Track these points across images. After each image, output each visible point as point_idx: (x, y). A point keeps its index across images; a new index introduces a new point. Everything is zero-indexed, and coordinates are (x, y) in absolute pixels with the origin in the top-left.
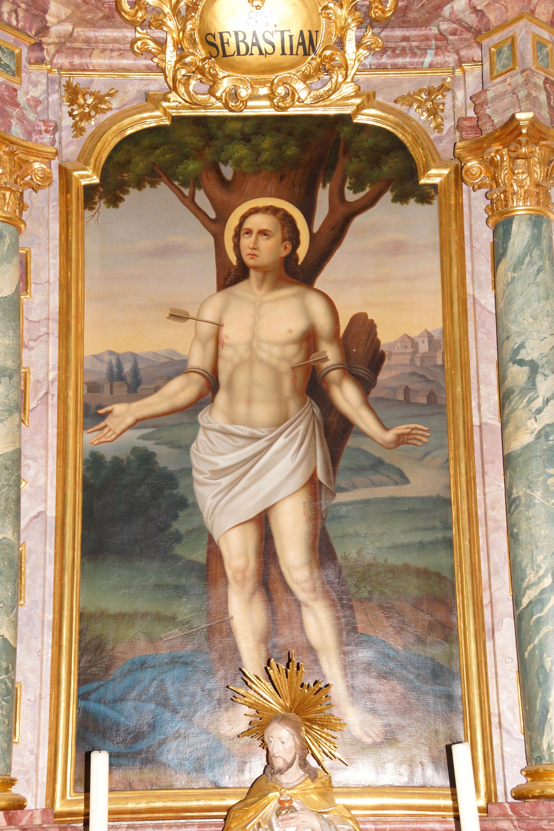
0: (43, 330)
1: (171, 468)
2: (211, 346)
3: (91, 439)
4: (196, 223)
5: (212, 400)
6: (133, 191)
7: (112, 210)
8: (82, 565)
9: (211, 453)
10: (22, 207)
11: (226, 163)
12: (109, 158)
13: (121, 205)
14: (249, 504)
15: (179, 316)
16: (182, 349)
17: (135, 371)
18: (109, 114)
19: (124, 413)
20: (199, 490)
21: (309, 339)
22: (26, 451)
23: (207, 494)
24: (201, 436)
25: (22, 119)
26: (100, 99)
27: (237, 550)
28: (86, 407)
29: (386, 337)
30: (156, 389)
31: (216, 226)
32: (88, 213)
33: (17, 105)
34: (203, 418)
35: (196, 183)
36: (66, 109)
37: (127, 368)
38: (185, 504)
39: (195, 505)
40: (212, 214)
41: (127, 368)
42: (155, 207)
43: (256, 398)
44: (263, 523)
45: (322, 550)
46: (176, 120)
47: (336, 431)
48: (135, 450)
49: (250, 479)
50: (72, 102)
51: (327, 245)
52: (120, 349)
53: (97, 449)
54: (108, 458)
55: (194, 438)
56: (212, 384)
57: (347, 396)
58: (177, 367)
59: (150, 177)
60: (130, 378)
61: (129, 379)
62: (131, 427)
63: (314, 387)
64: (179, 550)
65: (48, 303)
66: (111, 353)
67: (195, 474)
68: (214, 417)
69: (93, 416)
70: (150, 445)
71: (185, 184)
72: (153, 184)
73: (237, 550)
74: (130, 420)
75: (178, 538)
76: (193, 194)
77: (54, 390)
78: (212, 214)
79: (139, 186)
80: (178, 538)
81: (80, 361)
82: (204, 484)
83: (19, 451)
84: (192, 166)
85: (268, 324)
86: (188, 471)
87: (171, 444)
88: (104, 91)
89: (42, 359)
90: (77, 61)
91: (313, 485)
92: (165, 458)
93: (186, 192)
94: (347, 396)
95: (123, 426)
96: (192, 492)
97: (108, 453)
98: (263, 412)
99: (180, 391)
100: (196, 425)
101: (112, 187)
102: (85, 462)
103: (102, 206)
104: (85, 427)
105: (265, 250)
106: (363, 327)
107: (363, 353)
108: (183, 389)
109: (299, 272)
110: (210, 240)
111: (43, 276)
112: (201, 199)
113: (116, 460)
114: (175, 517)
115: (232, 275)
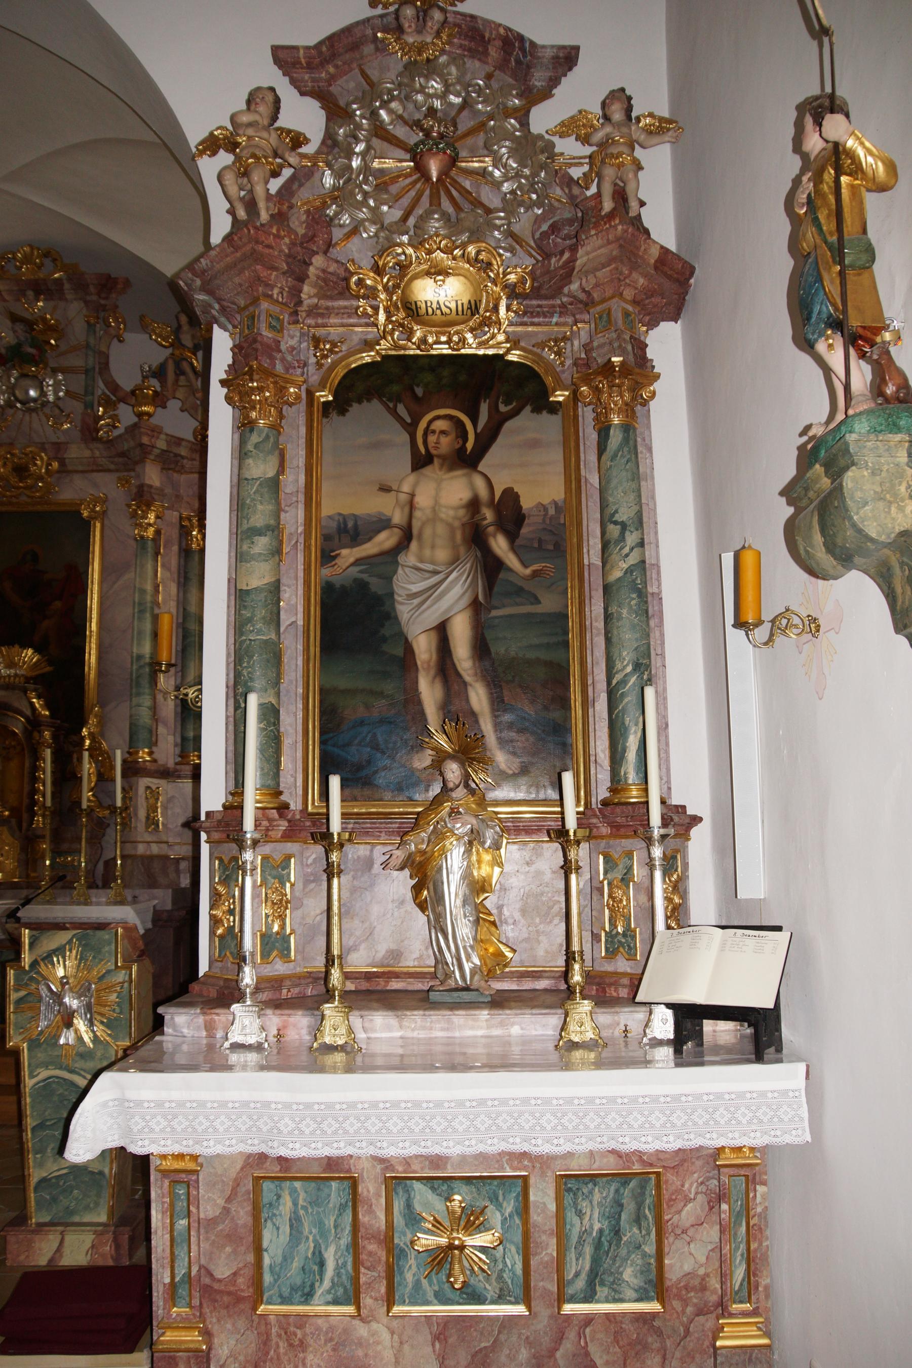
0: (295, 499)
1: (380, 593)
2: (407, 510)
3: (326, 572)
4: (398, 426)
5: (408, 546)
6: (355, 405)
7: (341, 418)
8: (321, 656)
9: (407, 582)
10: (281, 416)
11: (418, 386)
12: (340, 383)
13: (347, 414)
14: (431, 616)
15: (385, 489)
16: (387, 512)
17: (356, 526)
18: (340, 355)
19: (348, 555)
20: (399, 607)
21: (474, 505)
22: (284, 580)
23: (404, 611)
24: (400, 571)
25: (283, 360)
26: (334, 344)
27: (424, 648)
28: (323, 551)
29: (527, 503)
30: (370, 539)
31: (410, 429)
32: (325, 420)
33: (280, 351)
34: (401, 558)
35: (398, 399)
36: (312, 352)
37: (350, 524)
38: (389, 616)
39: (396, 618)
40: (409, 420)
41: (350, 524)
42: (370, 414)
43: (437, 545)
44: (442, 630)
45: (481, 647)
46: (386, 358)
47: (491, 567)
48: (355, 580)
49: (434, 602)
50: (316, 347)
52: (345, 512)
53: (330, 579)
54: (338, 586)
55: (395, 572)
56: (407, 535)
57: (500, 545)
58: (384, 524)
59: (367, 396)
60: (351, 531)
61: (351, 532)
62: (353, 564)
63: (476, 537)
64: (385, 648)
65: (297, 481)
66: (340, 514)
67: (396, 597)
68: (409, 558)
69: (327, 557)
70: (365, 577)
71: (390, 400)
72: (369, 400)
73: (424, 648)
74: (352, 560)
75: (384, 640)
76: (396, 406)
77: (301, 540)
78: (409, 420)
79: (360, 402)
80: (384, 640)
81: (318, 520)
82: (402, 604)
83: (278, 581)
84: (395, 388)
85: (446, 494)
86: (391, 594)
87: (379, 576)
88: (337, 339)
89: (294, 519)
90: (320, 321)
91: (476, 606)
92: (376, 586)
93: (391, 405)
94: (500, 545)
95: (347, 564)
96: (394, 609)
97: (337, 581)
98: (442, 555)
99: (385, 540)
100: (396, 563)
101: (340, 404)
102: (322, 589)
103: (334, 415)
104: (322, 565)
105: (445, 444)
106: (511, 496)
108: (388, 539)
109: (467, 460)
110: (406, 437)
111: (295, 463)
112: (401, 410)
113: (343, 586)
114: (383, 626)
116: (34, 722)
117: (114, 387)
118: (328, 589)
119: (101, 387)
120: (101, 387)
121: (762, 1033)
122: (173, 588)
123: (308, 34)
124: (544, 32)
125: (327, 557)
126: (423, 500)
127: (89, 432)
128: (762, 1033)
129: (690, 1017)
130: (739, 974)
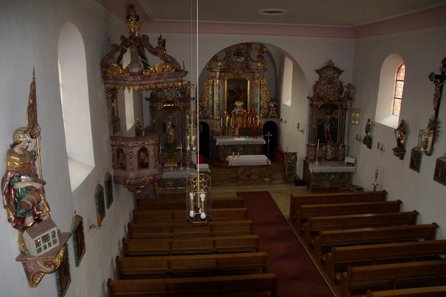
9: (325, 125)
19: (320, 122)
27: (326, 130)
44: (327, 129)
47: (332, 124)
49: (327, 127)
51: (332, 112)
56: (325, 121)
57: (333, 122)
60: (320, 120)
63: (331, 121)
73: (326, 130)
85: (329, 117)
91: (330, 127)
94: (333, 122)
99: (323, 121)
106: (334, 117)
107: (334, 119)
109: (330, 114)
115: (327, 114)
116: (244, 113)
117: (251, 59)
118: (318, 125)
119: (249, 59)
123: (318, 68)
124: (341, 68)
125: (318, 122)
127: (247, 67)
128: (353, 165)
129: (348, 163)
130: (352, 161)
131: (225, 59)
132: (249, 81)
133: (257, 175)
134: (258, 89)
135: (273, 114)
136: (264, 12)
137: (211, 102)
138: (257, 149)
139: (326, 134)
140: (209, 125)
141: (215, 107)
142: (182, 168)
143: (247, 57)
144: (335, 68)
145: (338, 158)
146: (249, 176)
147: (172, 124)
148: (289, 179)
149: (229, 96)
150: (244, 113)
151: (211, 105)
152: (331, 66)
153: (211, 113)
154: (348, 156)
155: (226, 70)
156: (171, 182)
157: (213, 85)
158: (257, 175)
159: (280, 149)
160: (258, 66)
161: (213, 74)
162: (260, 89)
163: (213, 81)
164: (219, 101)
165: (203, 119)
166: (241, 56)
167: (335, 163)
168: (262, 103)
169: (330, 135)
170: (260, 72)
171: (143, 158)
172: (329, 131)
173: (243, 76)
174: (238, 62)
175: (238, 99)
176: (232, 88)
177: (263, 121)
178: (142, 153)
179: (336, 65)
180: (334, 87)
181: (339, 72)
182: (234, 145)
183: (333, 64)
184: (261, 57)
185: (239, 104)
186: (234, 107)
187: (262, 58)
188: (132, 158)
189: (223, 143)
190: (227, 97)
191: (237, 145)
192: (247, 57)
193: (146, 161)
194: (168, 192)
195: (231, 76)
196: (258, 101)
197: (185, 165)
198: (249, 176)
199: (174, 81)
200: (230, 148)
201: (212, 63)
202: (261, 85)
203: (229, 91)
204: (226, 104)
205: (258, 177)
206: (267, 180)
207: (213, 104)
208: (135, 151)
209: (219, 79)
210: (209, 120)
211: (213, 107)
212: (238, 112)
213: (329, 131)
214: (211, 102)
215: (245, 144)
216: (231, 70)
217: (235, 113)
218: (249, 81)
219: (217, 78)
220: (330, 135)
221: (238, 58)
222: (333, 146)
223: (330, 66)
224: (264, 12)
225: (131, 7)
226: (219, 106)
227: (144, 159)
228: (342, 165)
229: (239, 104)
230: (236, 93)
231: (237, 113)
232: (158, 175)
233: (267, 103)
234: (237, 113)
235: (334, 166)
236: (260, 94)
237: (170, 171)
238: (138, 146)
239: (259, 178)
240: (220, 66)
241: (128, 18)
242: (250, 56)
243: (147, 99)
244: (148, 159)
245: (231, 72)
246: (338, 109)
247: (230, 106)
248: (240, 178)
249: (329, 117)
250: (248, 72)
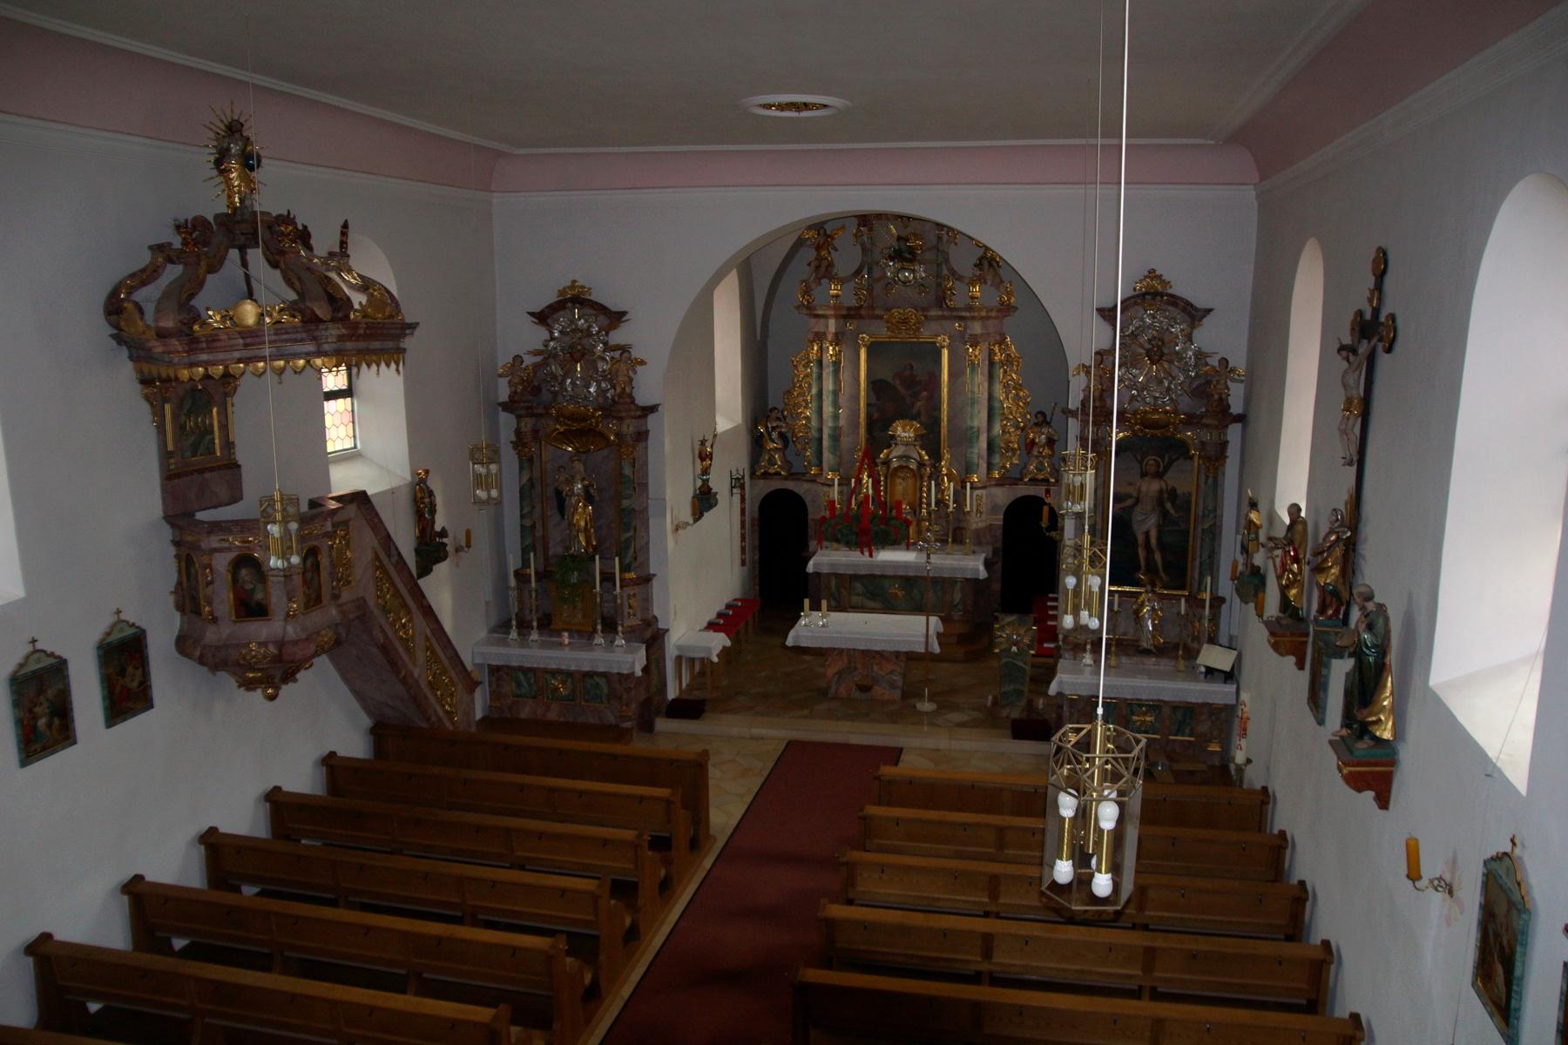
9: (1137, 517)
14: (1145, 528)
21: (1161, 491)
23: (1135, 527)
29: (1179, 492)
44: (1147, 534)
45: (1159, 539)
47: (1165, 514)
49: (1146, 524)
56: (1138, 501)
57: (1168, 506)
58: (1130, 496)
63: (1160, 502)
68: (1138, 509)
73: (1141, 538)
85: (1152, 487)
94: (1168, 506)
99: (1129, 502)
105: (1152, 469)
107: (1173, 494)
109: (1159, 475)
115: (1144, 475)
116: (921, 464)
117: (953, 272)
119: (945, 272)
120: (945, 272)
121: (1229, 676)
122: (986, 384)
124: (1200, 301)
126: (1144, 489)
127: (941, 300)
129: (1210, 671)
131: (858, 272)
132: (945, 352)
133: (893, 686)
134: (981, 379)
135: (1040, 469)
136: (768, 106)
137: (814, 423)
138: (957, 597)
139: (1142, 553)
140: (807, 500)
141: (826, 443)
142: (599, 639)
143: (939, 265)
144: (1175, 301)
145: (1178, 650)
146: (865, 689)
147: (586, 489)
148: (1005, 713)
149: (874, 401)
150: (921, 464)
151: (814, 433)
152: (1156, 294)
153: (814, 461)
154: (1213, 640)
155: (863, 312)
156: (564, 683)
157: (820, 362)
158: (893, 686)
159: (1056, 600)
160: (973, 298)
161: (819, 326)
162: (991, 377)
163: (821, 348)
164: (836, 417)
165: (786, 478)
166: (911, 261)
167: (1165, 665)
168: (997, 429)
169: (1158, 557)
170: (988, 318)
171: (248, 587)
172: (1153, 541)
173: (925, 334)
174: (905, 283)
175: (905, 414)
176: (886, 374)
177: (1003, 496)
178: (244, 572)
179: (1178, 289)
180: (1175, 371)
181: (1194, 315)
182: (873, 576)
183: (1166, 284)
184: (986, 263)
185: (904, 431)
186: (890, 441)
187: (991, 265)
188: (212, 582)
189: (833, 565)
190: (868, 405)
191: (883, 576)
192: (939, 265)
193: (259, 596)
194: (553, 715)
195: (882, 332)
196: (979, 419)
197: (610, 627)
198: (865, 689)
199: (308, 354)
200: (859, 586)
201: (813, 285)
202: (992, 364)
203: (876, 385)
204: (862, 431)
205: (897, 694)
206: (926, 706)
207: (820, 430)
208: (222, 562)
209: (837, 341)
210: (806, 486)
211: (820, 440)
212: (900, 458)
213: (1153, 541)
214: (814, 423)
215: (878, 573)
216: (877, 312)
217: (887, 463)
218: (945, 352)
219: (830, 337)
220: (1158, 557)
221: (903, 269)
222: (1162, 597)
223: (1152, 294)
224: (768, 106)
225: (234, 129)
226: (836, 437)
227: (253, 591)
228: (1191, 673)
229: (904, 431)
230: (902, 392)
231: (895, 463)
232: (295, 643)
233: (1023, 429)
234: (895, 463)
235: (1151, 675)
236: (991, 398)
237: (561, 644)
238: (229, 549)
239: (905, 695)
240: (837, 296)
241: (220, 162)
242: (947, 260)
243: (506, 407)
244: (265, 590)
245: (880, 317)
246: (1191, 458)
247: (878, 434)
248: (833, 689)
249: (1152, 487)
250: (943, 317)
